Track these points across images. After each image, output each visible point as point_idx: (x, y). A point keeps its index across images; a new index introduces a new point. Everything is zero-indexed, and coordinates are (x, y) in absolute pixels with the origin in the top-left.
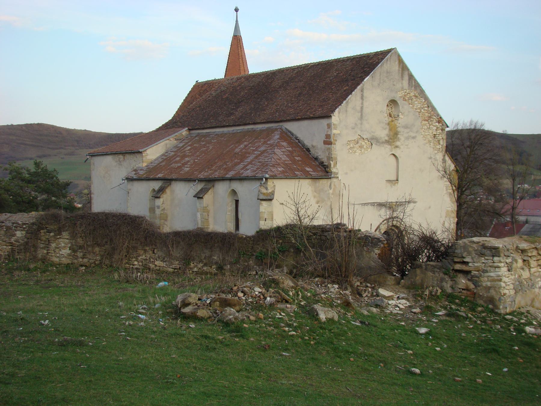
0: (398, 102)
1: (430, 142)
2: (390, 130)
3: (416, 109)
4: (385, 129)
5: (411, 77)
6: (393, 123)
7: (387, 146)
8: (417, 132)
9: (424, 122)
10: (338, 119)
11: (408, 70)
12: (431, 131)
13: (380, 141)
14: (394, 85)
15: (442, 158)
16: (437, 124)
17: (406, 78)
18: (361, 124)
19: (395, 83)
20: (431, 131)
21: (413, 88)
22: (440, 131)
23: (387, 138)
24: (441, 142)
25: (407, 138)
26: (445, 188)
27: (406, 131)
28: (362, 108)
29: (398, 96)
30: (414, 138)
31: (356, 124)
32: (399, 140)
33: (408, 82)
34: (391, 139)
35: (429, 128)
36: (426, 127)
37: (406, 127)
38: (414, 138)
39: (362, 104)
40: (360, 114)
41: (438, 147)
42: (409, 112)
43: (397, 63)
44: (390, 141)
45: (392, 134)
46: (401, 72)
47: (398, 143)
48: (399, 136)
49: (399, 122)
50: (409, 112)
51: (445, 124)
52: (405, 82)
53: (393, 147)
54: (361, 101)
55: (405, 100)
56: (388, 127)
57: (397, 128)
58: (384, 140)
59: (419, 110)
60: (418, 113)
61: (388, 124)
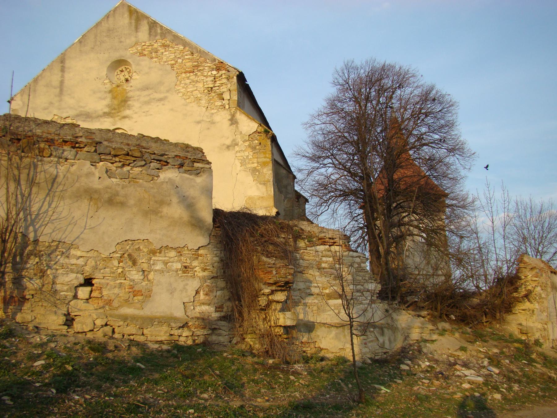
0: (129, 60)
1: (198, 99)
2: (114, 98)
3: (166, 62)
4: (104, 99)
5: (153, 25)
6: (120, 88)
7: (106, 119)
8: (168, 91)
9: (184, 75)
10: (20, 103)
11: (147, 18)
12: (201, 85)
13: (94, 115)
14: (121, 42)
15: (230, 117)
16: (214, 72)
17: (144, 27)
18: (61, 100)
19: (123, 39)
20: (201, 85)
21: (158, 37)
22: (225, 81)
23: (106, 110)
24: (226, 96)
25: (147, 103)
26: (238, 163)
27: (146, 93)
28: (62, 82)
29: (127, 54)
30: (160, 100)
31: (51, 103)
32: (129, 107)
33: (147, 32)
34: (115, 109)
35: (197, 81)
36: (188, 81)
37: (146, 88)
38: (160, 100)
39: (63, 76)
40: (58, 90)
41: (219, 103)
42: (150, 68)
43: (126, 15)
44: (113, 111)
45: (116, 102)
46: (133, 24)
47: (127, 112)
48: (129, 103)
49: (131, 84)
50: (150, 68)
51: (230, 69)
52: (143, 33)
53: (117, 119)
54: (60, 74)
55: (145, 55)
56: (109, 96)
57: (127, 93)
58: (101, 113)
59: (173, 62)
60: (169, 67)
61: (110, 92)
